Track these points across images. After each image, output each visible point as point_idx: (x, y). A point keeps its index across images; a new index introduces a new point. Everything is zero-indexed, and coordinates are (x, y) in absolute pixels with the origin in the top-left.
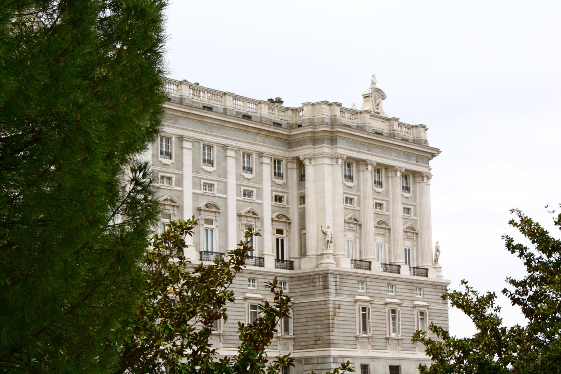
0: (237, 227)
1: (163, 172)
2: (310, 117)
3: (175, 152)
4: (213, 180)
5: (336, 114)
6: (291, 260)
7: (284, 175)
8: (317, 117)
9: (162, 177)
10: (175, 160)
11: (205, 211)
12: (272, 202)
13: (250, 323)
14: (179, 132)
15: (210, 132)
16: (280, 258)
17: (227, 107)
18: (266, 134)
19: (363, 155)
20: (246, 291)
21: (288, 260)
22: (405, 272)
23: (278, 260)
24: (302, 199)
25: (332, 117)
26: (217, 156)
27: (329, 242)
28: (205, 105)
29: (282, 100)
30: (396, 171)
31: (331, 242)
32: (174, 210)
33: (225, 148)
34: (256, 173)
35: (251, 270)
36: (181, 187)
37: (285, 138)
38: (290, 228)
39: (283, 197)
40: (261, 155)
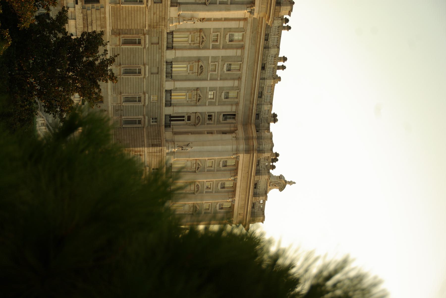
0: (189, 88)
1: (220, 36)
2: (263, 137)
3: (234, 44)
4: (218, 71)
5: (265, 154)
6: (171, 126)
7: (225, 122)
8: (263, 141)
9: (217, 36)
10: (229, 44)
11: (198, 65)
12: (208, 113)
13: (111, 56)
14: (247, 46)
15: (249, 68)
16: (172, 119)
17: (266, 80)
18: (251, 108)
19: (241, 173)
20: (149, 94)
21: (171, 124)
23: (171, 116)
24: (211, 133)
25: (263, 151)
26: (234, 74)
27: (182, 148)
28: (266, 66)
29: (276, 123)
31: (182, 149)
32: (197, 43)
33: (239, 79)
34: (225, 101)
35: (163, 97)
36: (212, 49)
37: (249, 122)
38: (192, 125)
39: (212, 121)
40: (237, 104)
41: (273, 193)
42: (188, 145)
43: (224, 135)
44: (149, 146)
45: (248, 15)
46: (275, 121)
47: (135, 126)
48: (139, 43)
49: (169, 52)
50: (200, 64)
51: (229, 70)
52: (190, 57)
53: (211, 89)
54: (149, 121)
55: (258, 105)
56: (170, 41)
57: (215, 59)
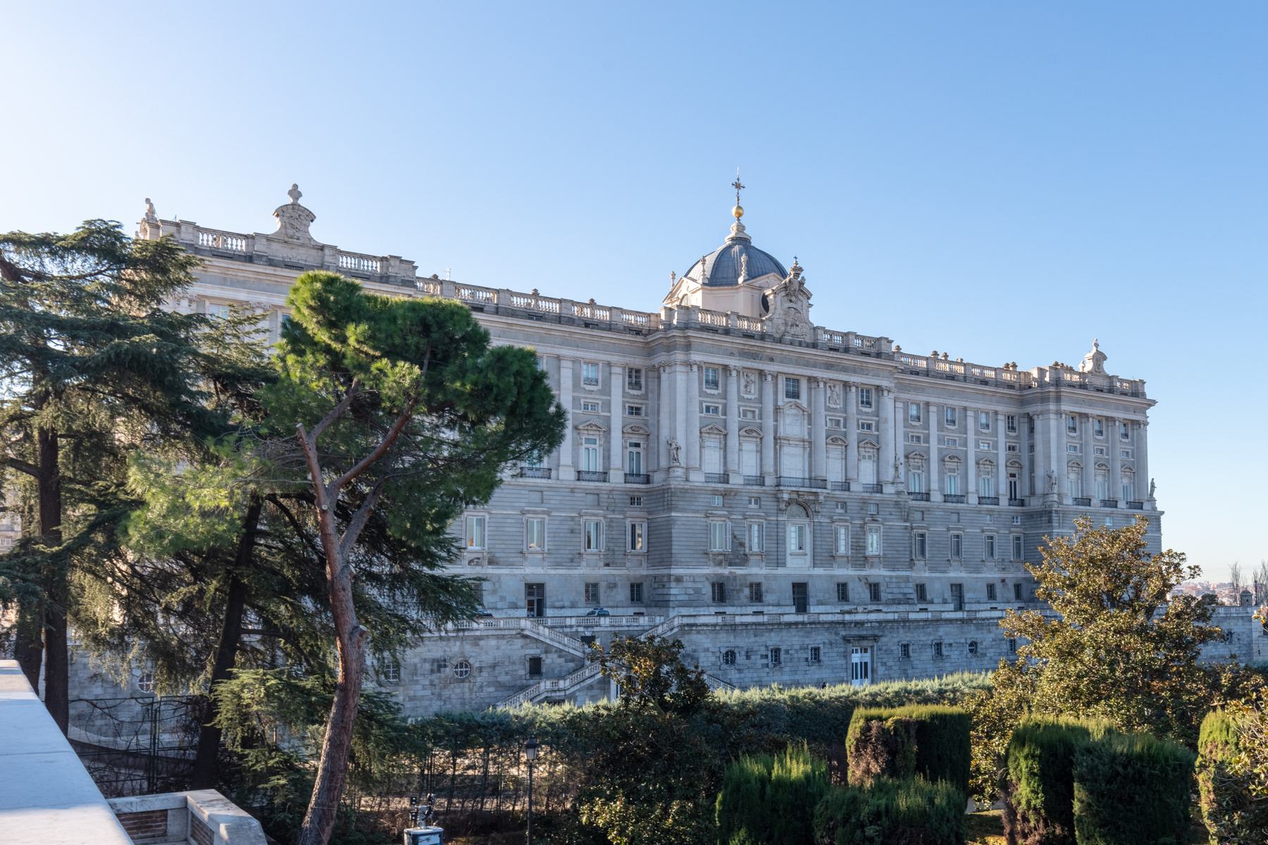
9: (912, 437)
22: (1122, 505)
23: (1011, 499)
24: (1032, 448)
30: (1115, 421)
33: (965, 409)
40: (996, 413)
41: (1109, 368)
42: (1050, 477)
43: (1036, 430)
44: (1052, 527)
45: (892, 396)
46: (1014, 366)
47: (1022, 545)
48: (922, 535)
49: (932, 499)
50: (947, 459)
51: (953, 422)
52: (939, 472)
53: (977, 446)
54: (1016, 527)
55: (996, 386)
56: (919, 497)
57: (940, 441)
